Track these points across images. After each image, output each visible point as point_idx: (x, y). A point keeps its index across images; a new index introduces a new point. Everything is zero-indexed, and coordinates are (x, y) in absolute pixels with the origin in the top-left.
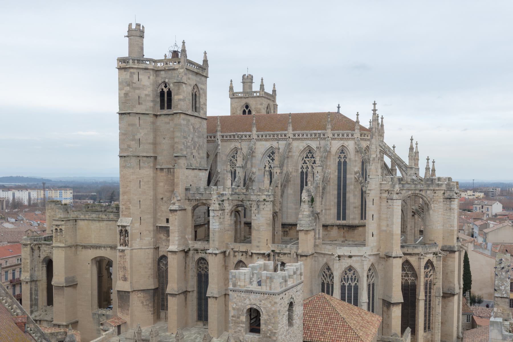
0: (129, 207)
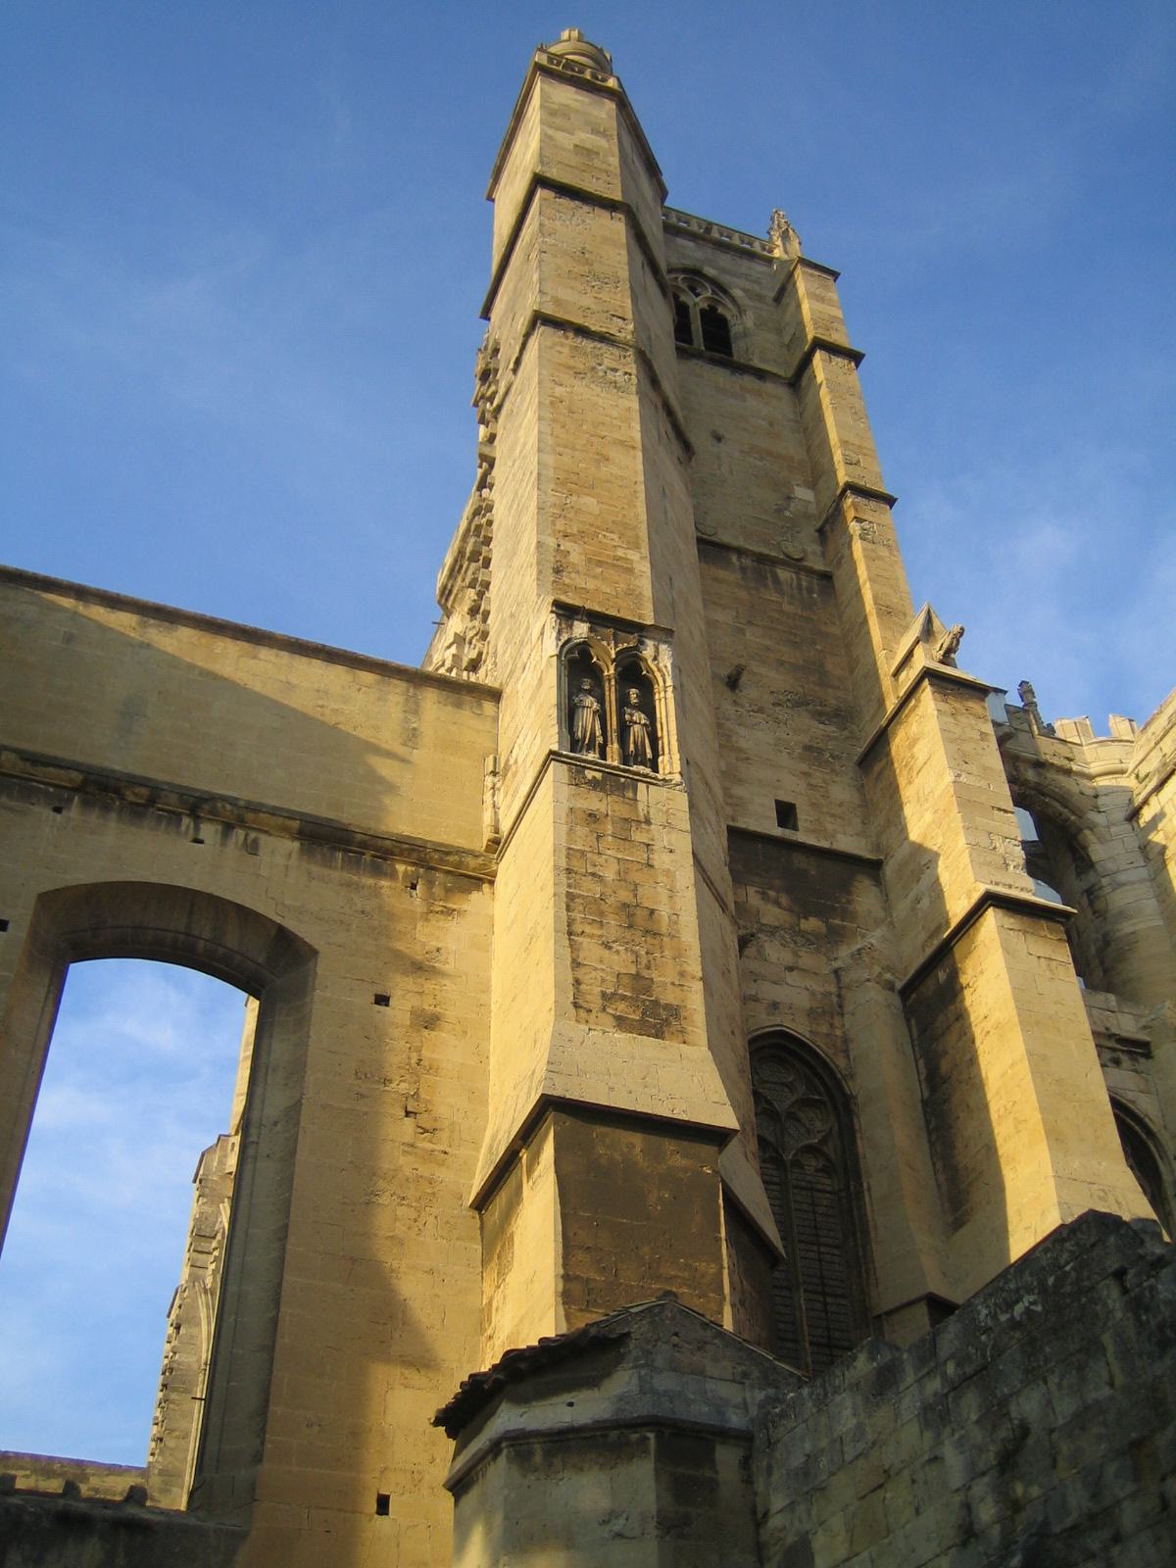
0: (630, 561)
